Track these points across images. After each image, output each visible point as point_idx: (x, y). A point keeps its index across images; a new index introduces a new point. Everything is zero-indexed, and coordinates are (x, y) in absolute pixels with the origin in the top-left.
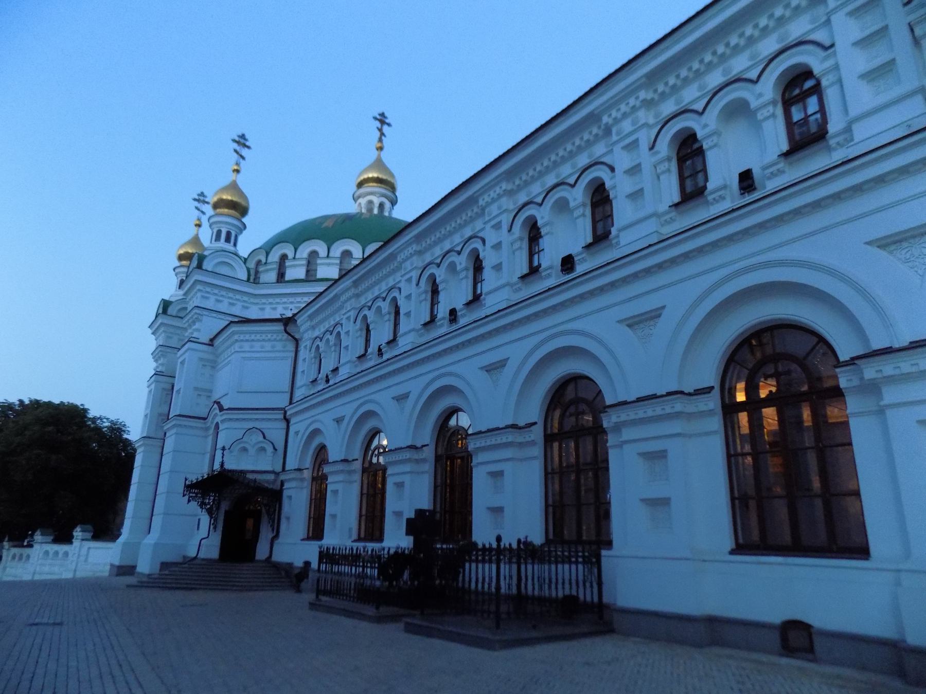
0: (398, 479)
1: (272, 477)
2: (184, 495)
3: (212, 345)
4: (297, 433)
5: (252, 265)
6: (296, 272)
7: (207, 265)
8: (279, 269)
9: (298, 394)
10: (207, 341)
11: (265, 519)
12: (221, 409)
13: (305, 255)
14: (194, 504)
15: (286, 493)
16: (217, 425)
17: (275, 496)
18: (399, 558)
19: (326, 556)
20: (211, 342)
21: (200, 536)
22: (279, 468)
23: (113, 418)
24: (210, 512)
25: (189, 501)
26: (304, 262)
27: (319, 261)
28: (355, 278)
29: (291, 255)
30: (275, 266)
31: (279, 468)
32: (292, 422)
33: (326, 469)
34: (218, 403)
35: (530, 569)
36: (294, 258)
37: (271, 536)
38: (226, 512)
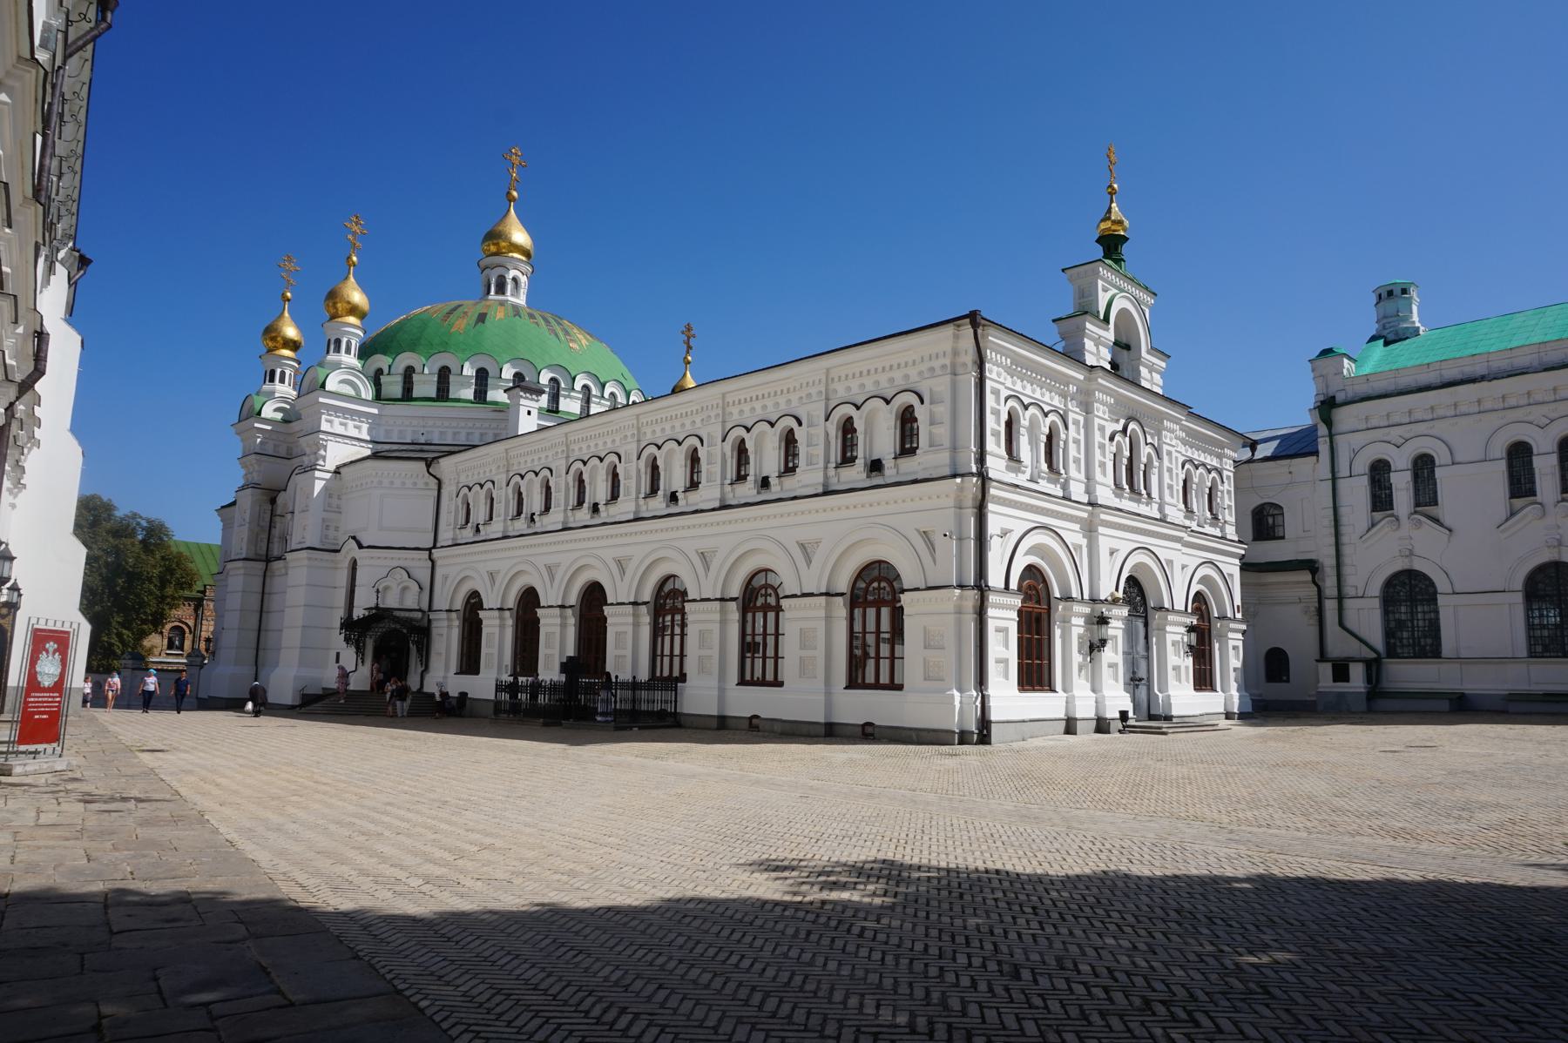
0: (550, 630)
1: (419, 615)
4: (446, 578)
6: (425, 385)
7: (331, 385)
9: (445, 536)
10: (333, 468)
12: (360, 546)
13: (436, 370)
15: (434, 632)
16: (354, 565)
18: (554, 687)
19: (499, 687)
20: (337, 472)
22: (425, 607)
23: (153, 515)
27: (452, 378)
30: (400, 379)
31: (425, 607)
32: (439, 563)
33: (482, 614)
34: (354, 538)
35: (644, 694)
37: (420, 669)
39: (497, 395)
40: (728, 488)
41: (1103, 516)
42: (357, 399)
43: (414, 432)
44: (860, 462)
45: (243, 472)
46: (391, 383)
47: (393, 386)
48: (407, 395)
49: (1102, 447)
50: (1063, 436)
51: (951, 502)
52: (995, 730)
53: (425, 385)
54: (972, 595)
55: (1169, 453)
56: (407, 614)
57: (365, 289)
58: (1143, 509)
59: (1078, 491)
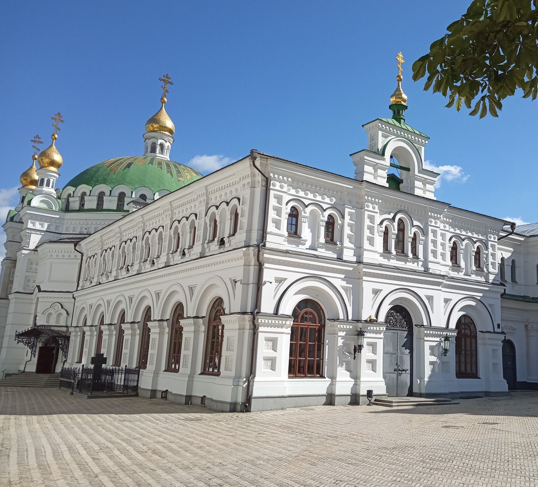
2: (15, 340)
3: (37, 251)
5: (65, 196)
8: (81, 201)
11: (61, 352)
12: (40, 291)
13: (97, 194)
14: (21, 344)
17: (67, 338)
21: (27, 359)
24: (32, 348)
25: (18, 343)
26: (96, 198)
28: (101, 235)
29: (88, 194)
30: (78, 199)
34: (38, 287)
36: (90, 195)
38: (40, 347)
39: (126, 208)
40: (171, 256)
41: (364, 270)
42: (50, 210)
43: (81, 228)
44: (216, 239)
45: (6, 251)
46: (74, 201)
47: (75, 204)
48: (81, 209)
49: (371, 229)
50: (340, 222)
51: (242, 262)
52: (253, 401)
53: (91, 203)
54: (248, 317)
55: (435, 232)
56: (58, 329)
57: (61, 152)
58: (410, 265)
59: (349, 255)
